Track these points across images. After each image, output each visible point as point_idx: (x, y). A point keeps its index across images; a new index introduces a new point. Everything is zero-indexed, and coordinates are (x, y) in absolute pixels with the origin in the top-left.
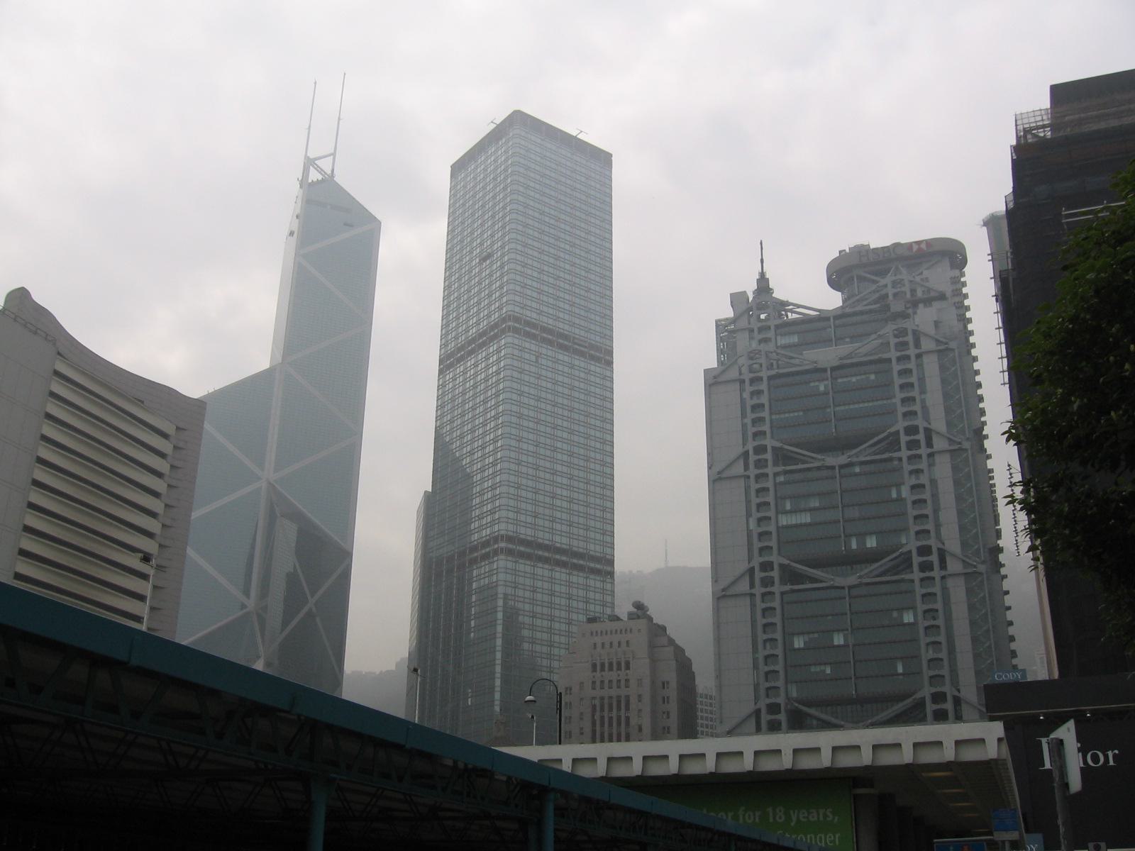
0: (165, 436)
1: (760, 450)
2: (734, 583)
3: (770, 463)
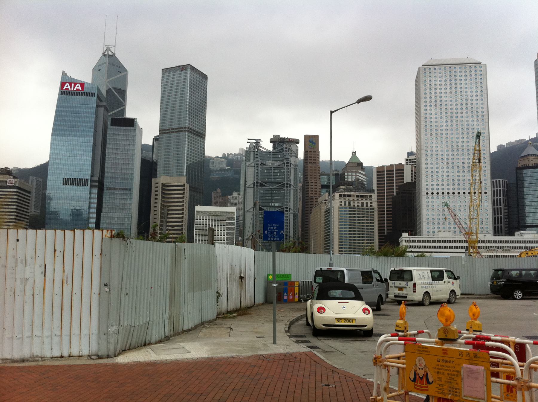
1: (257, 182)
2: (250, 209)
3: (259, 186)
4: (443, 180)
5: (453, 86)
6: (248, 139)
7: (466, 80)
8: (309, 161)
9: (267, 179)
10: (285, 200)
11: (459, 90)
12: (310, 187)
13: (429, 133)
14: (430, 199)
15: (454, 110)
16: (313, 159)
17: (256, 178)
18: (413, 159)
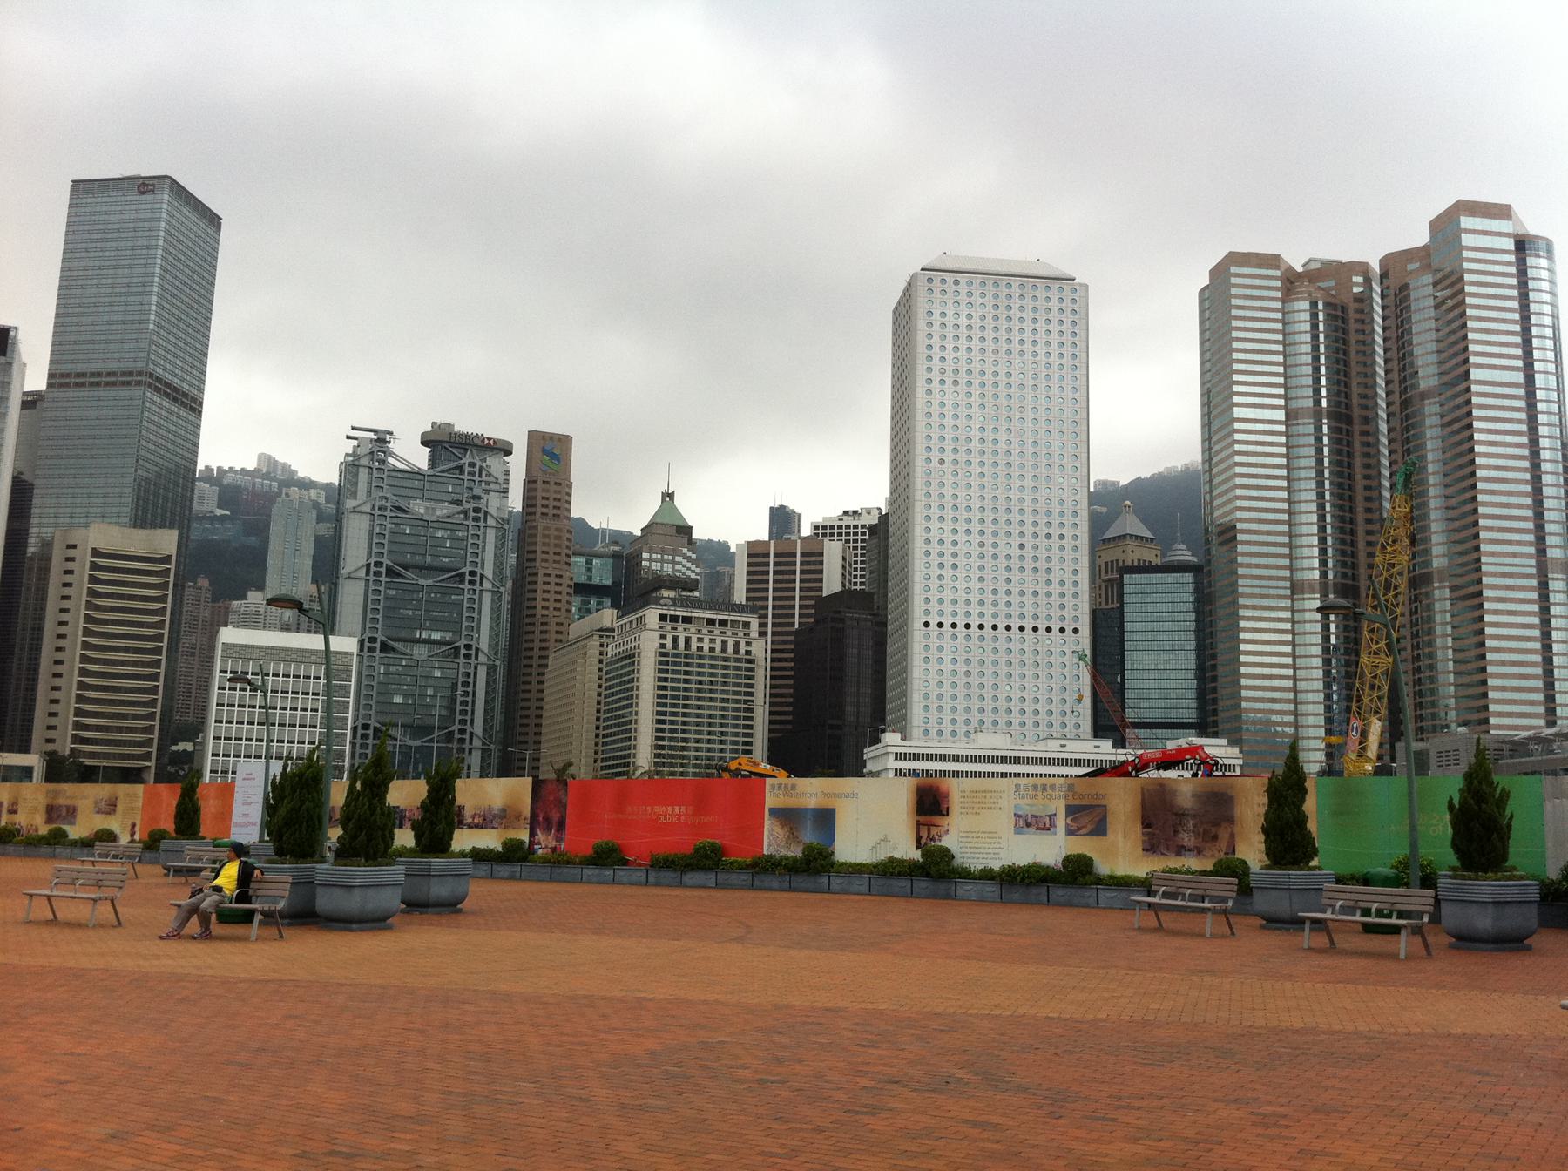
1: (378, 564)
3: (384, 575)
4: (968, 591)
5: (1003, 335)
6: (353, 428)
7: (1035, 320)
8: (539, 510)
9: (409, 556)
10: (465, 623)
11: (1016, 346)
12: (540, 587)
13: (935, 456)
14: (934, 642)
15: (1002, 400)
16: (552, 503)
17: (375, 549)
18: (848, 527)
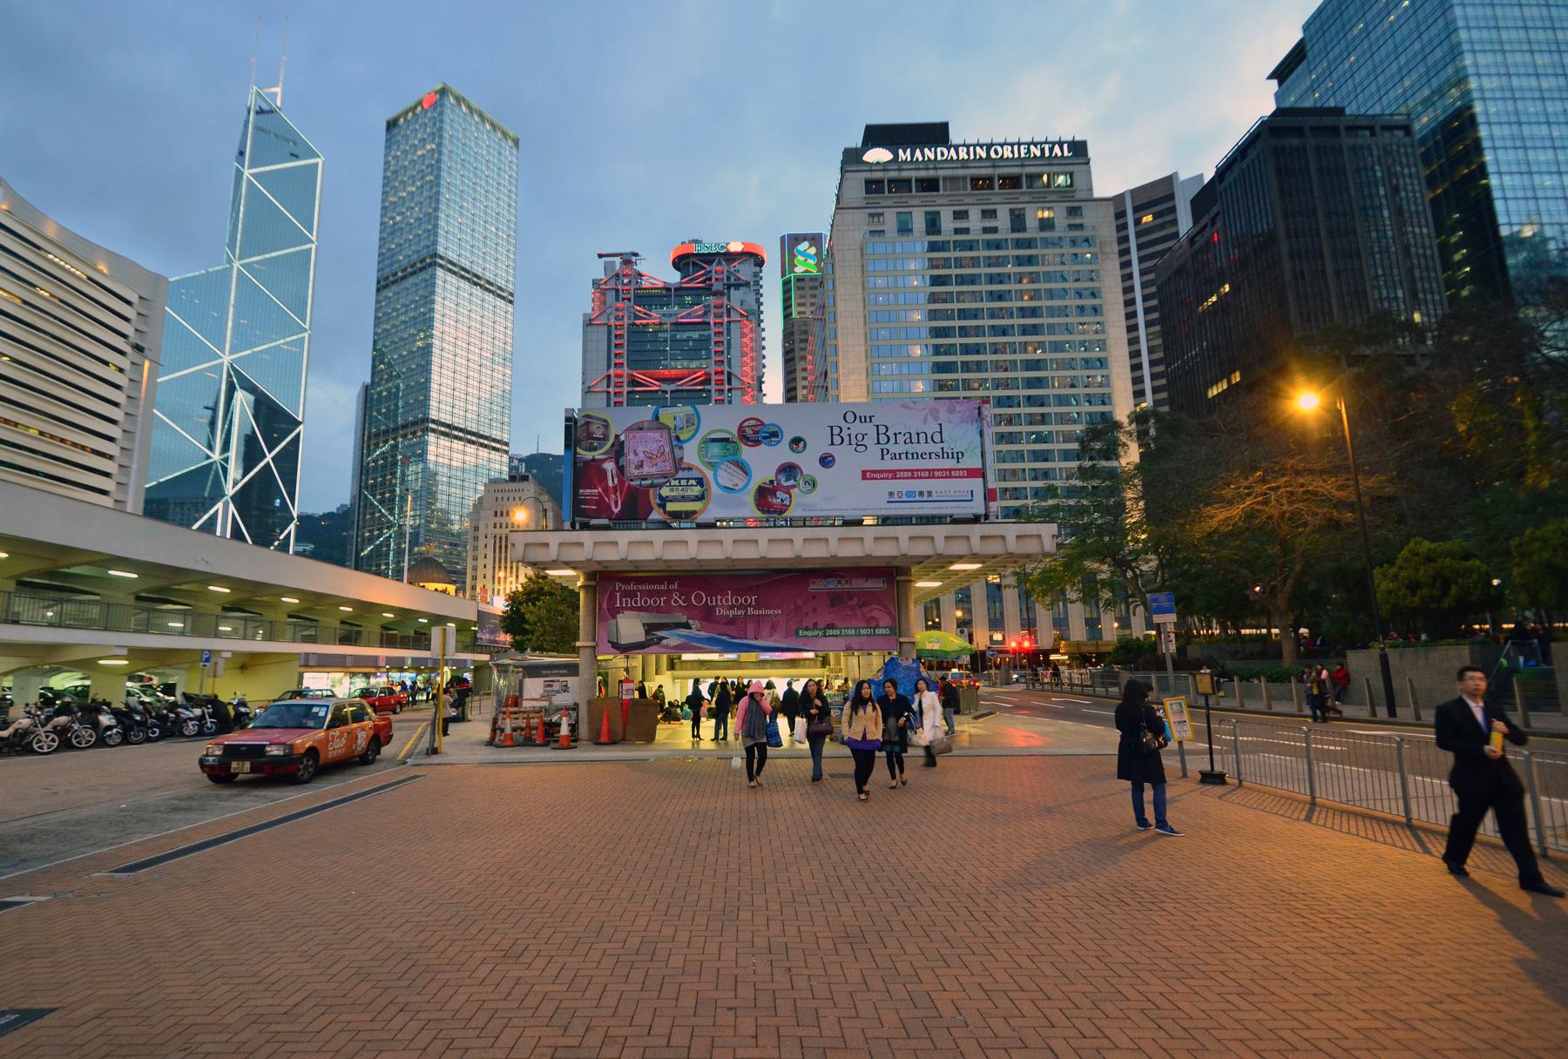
0: (129, 303)
6: (600, 256)
